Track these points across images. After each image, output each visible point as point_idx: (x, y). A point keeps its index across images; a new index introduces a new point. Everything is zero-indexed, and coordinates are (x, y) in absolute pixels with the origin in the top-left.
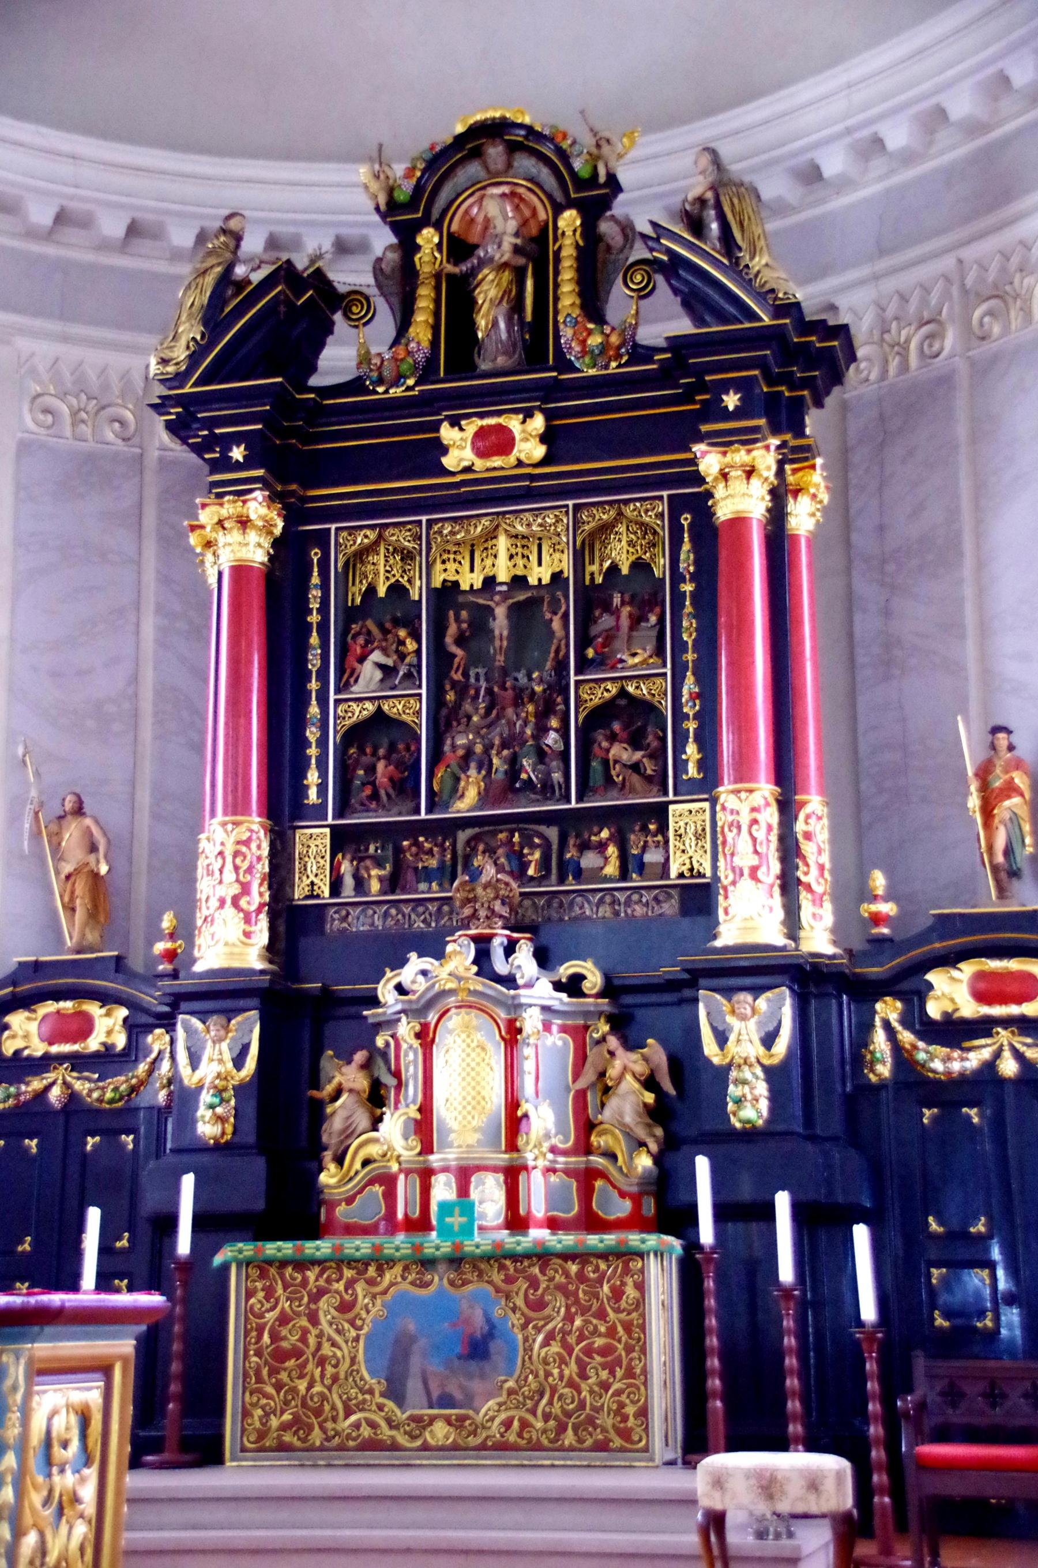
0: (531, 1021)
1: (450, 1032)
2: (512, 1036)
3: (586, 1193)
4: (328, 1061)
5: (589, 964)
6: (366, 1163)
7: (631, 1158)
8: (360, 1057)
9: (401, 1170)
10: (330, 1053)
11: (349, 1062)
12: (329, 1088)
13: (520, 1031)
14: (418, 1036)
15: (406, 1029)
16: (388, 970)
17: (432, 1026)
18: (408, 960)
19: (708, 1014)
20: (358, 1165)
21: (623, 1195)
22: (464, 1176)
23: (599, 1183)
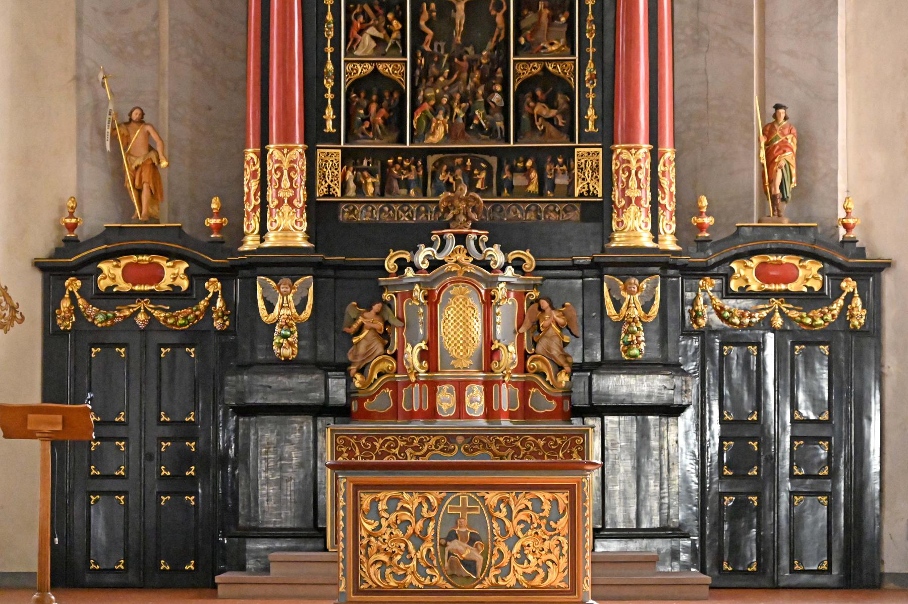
0: (501, 291)
1: (452, 296)
2: (489, 301)
3: (525, 396)
4: (351, 309)
5: (528, 253)
6: (380, 375)
7: (556, 377)
8: (377, 307)
9: (416, 382)
10: (355, 303)
11: (369, 309)
12: (355, 326)
13: (494, 297)
14: (425, 298)
15: (418, 293)
16: (391, 250)
17: (437, 292)
18: (418, 248)
19: (609, 290)
20: (375, 376)
21: (550, 398)
22: (460, 387)
23: (533, 390)
